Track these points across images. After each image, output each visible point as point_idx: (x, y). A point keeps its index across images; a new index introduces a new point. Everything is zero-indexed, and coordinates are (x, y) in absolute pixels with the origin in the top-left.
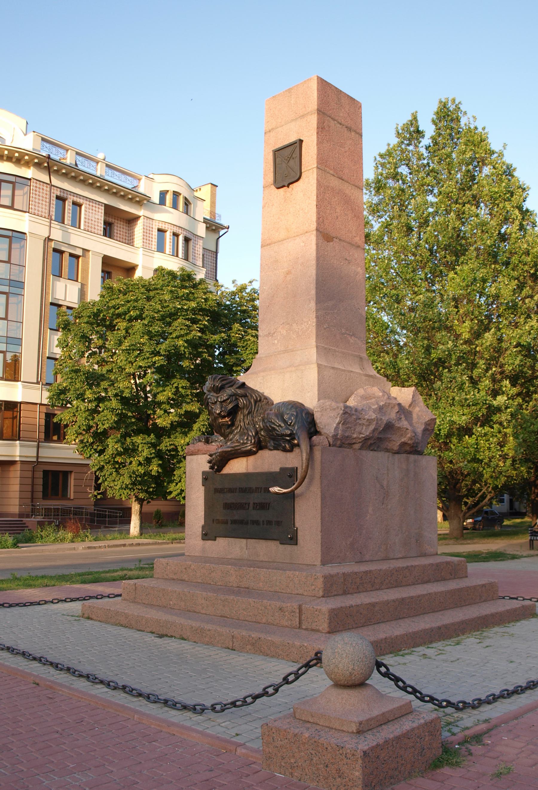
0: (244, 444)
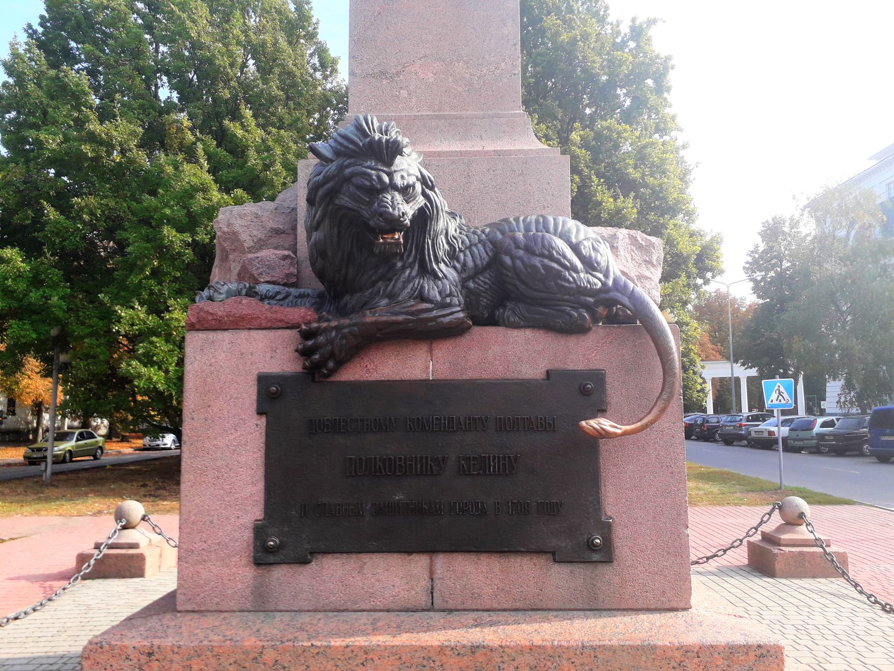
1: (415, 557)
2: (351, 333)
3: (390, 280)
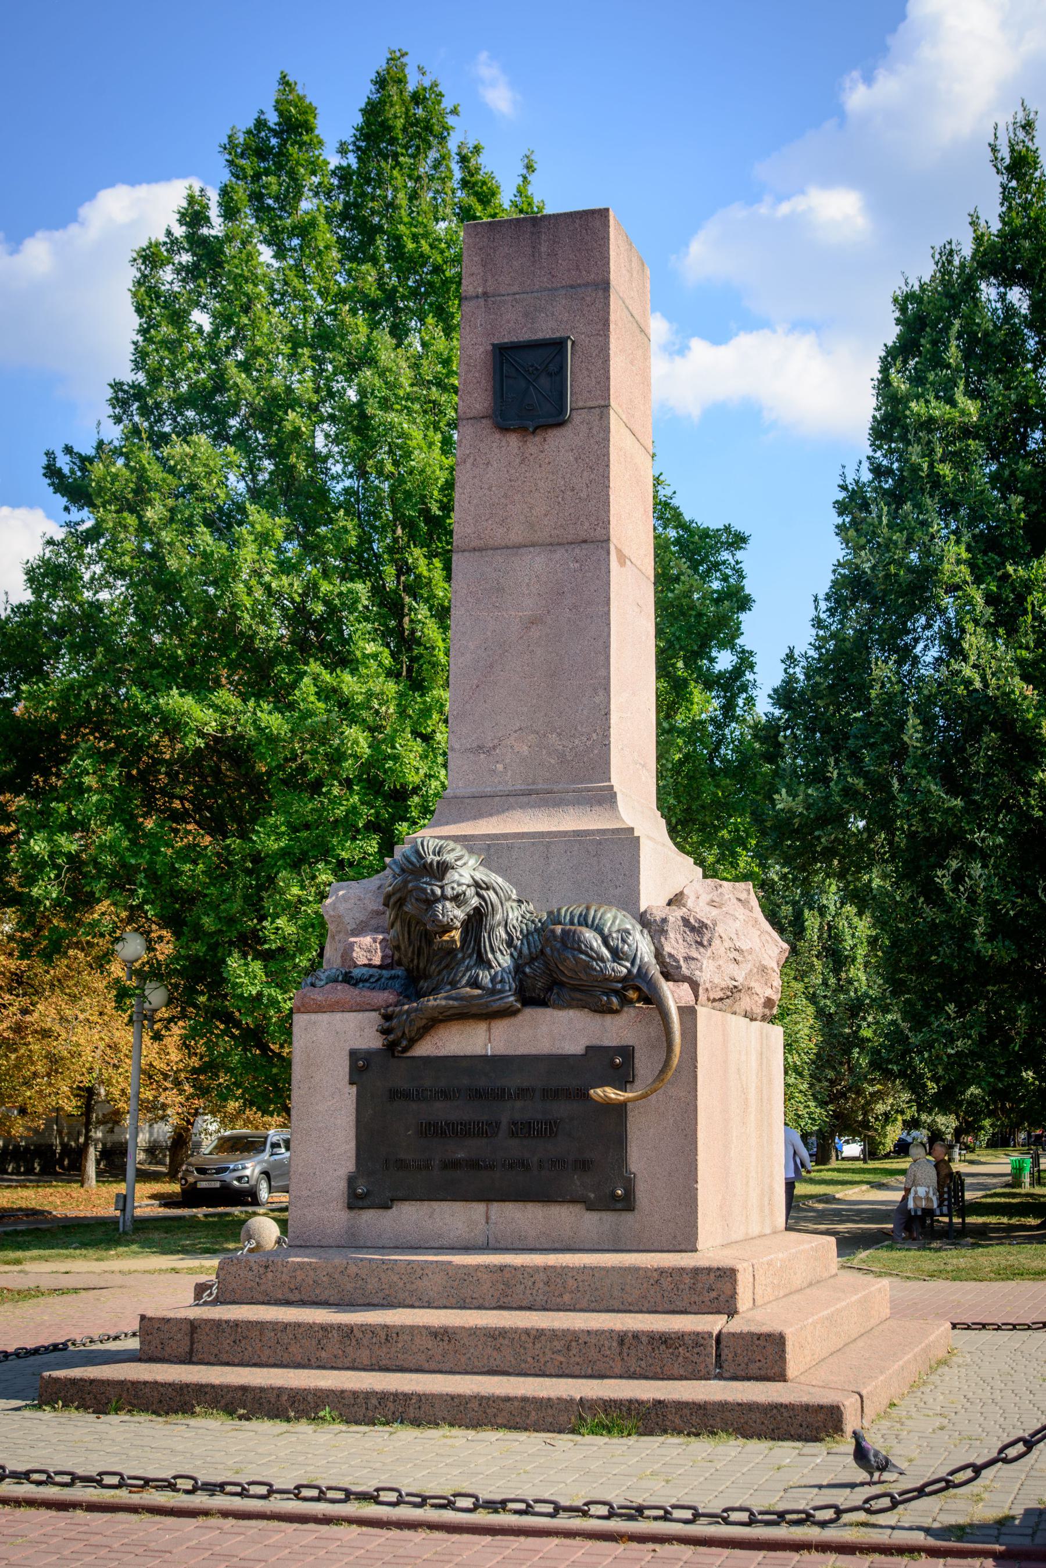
0: (493, 992)
1: (475, 1205)
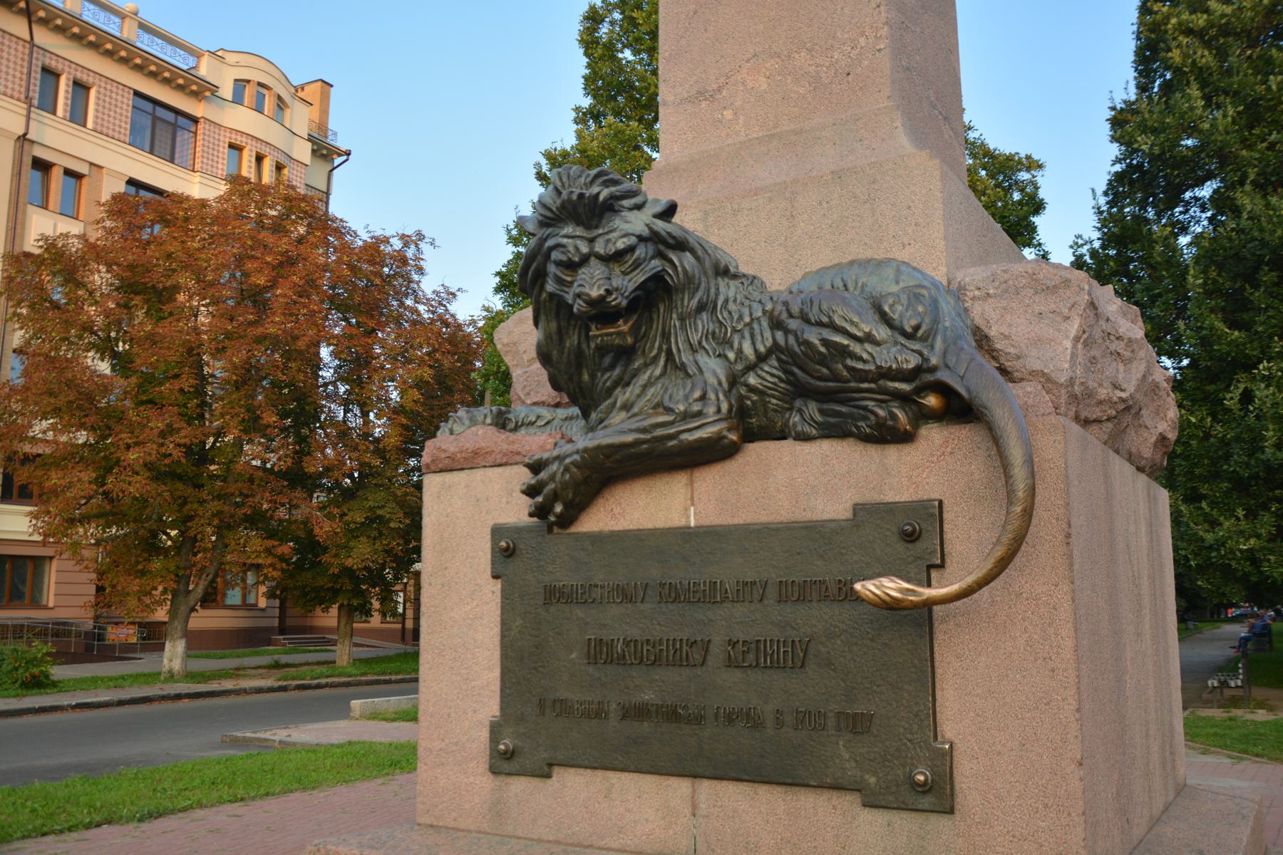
0: (686, 416)
1: (673, 782)
2: (572, 463)
3: (628, 384)
